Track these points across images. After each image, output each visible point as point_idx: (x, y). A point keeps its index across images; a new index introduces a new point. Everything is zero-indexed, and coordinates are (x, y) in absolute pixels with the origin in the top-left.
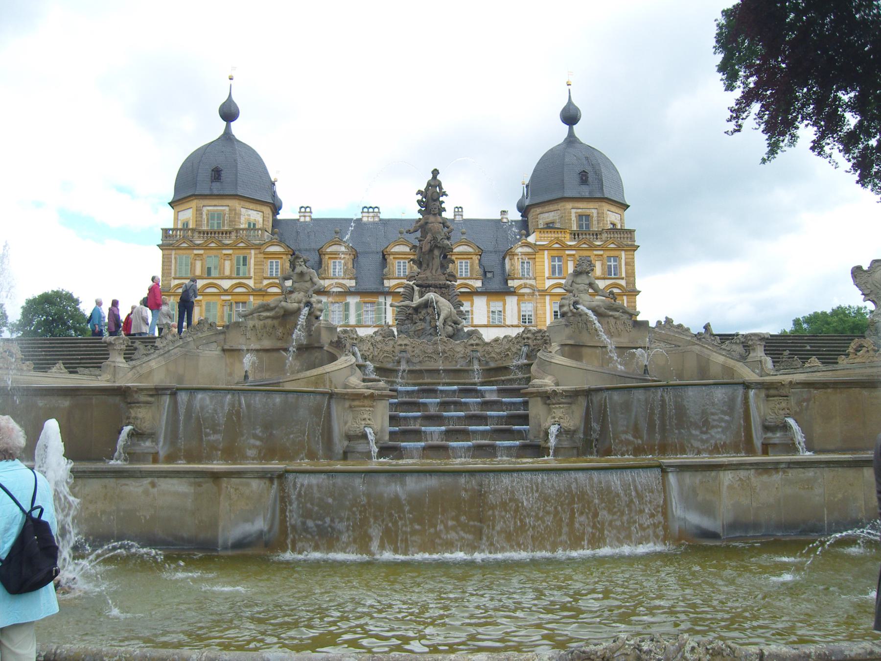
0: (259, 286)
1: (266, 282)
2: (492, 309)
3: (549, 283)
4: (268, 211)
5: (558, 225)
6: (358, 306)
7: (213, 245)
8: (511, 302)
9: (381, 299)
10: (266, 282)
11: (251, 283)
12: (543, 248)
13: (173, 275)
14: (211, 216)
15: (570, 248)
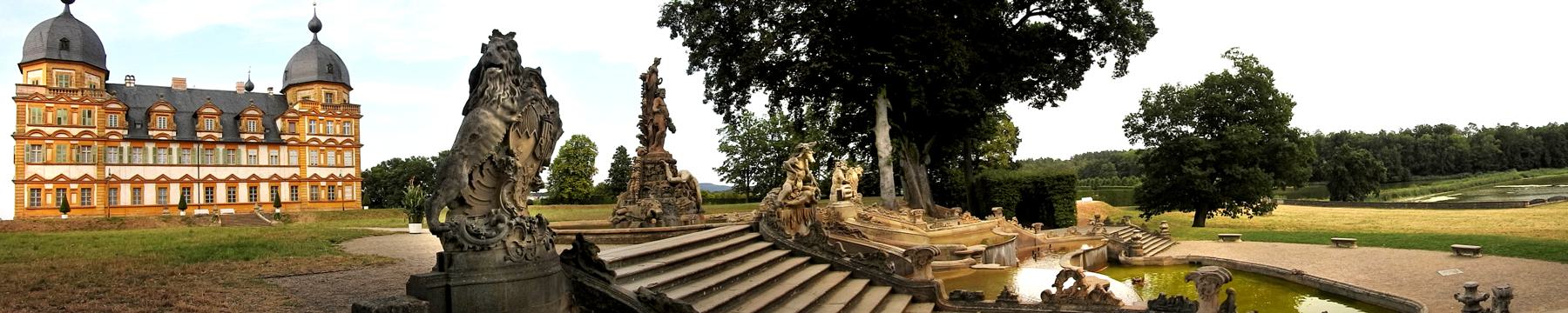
0: (102, 134)
1: (107, 131)
2: (271, 154)
3: (308, 138)
4: (103, 76)
5: (312, 99)
6: (178, 149)
7: (62, 100)
8: (284, 150)
9: (195, 146)
10: (107, 131)
11: (95, 131)
12: (304, 114)
13: (27, 122)
14: (60, 77)
15: (321, 115)
